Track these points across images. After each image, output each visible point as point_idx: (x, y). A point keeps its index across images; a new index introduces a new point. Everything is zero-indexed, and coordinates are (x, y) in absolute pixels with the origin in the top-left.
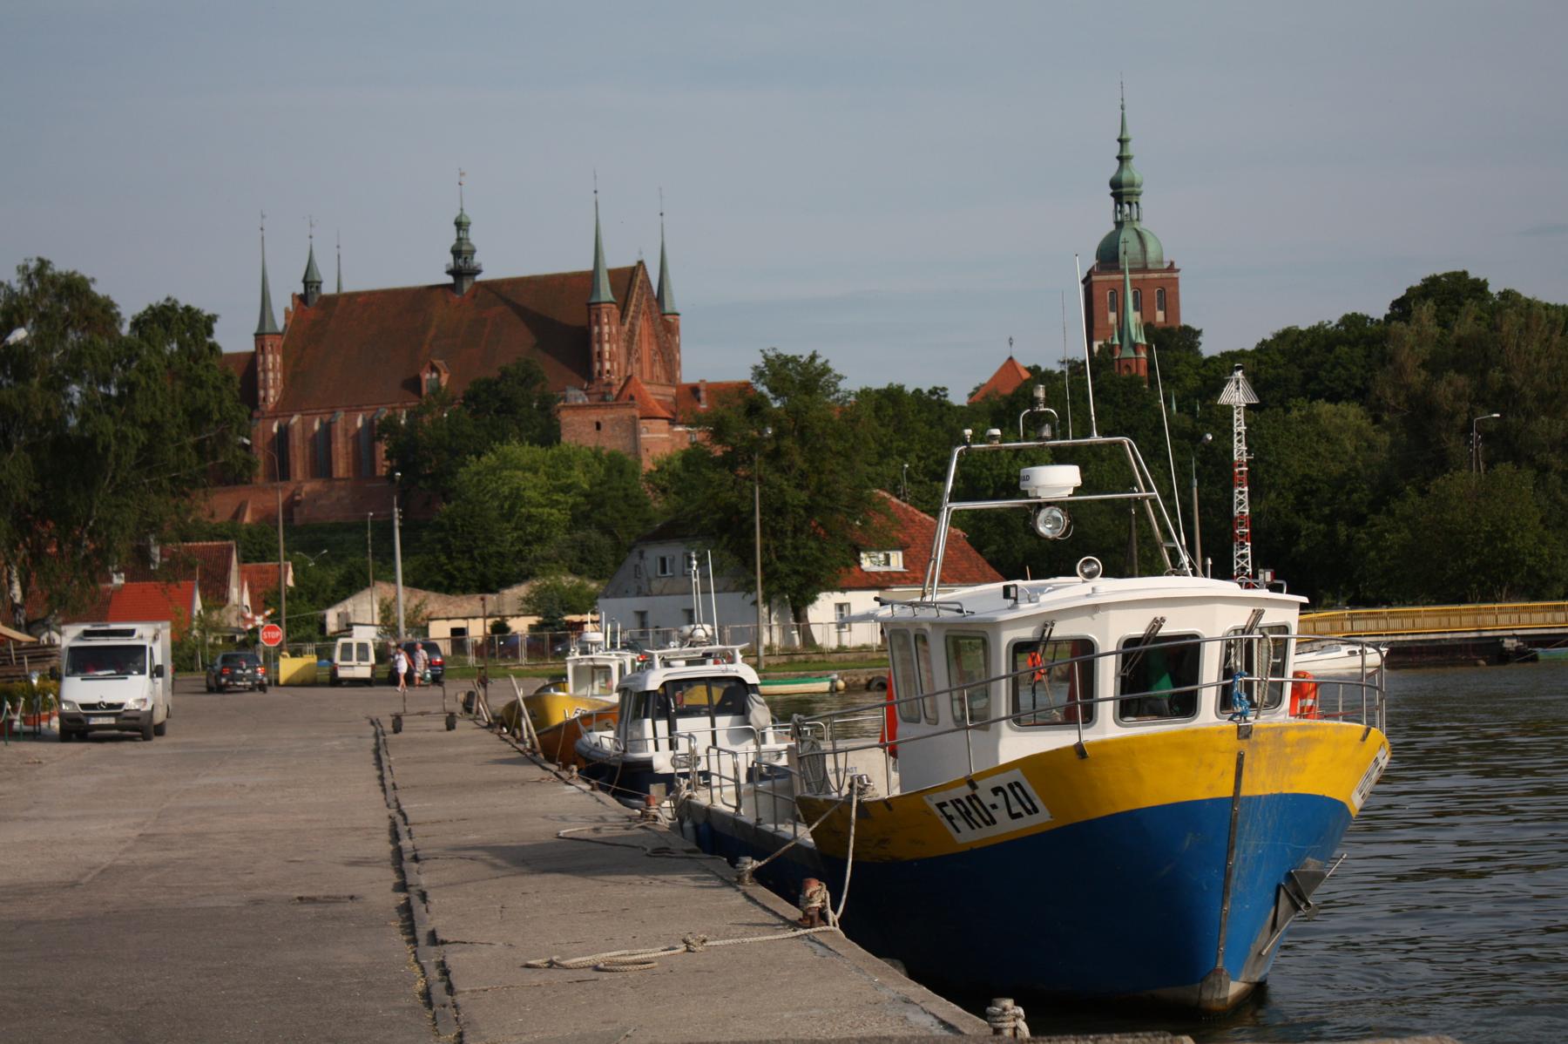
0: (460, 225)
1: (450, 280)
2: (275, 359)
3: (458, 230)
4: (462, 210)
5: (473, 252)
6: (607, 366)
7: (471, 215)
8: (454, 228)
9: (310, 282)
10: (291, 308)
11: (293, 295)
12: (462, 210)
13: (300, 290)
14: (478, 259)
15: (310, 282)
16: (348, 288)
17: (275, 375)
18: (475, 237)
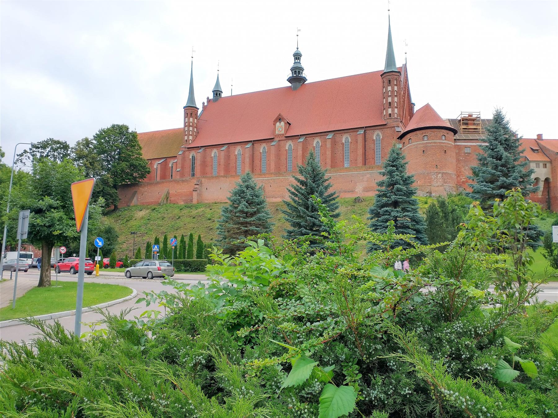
0: (297, 56)
1: (289, 84)
2: (194, 120)
3: (296, 59)
4: (297, 48)
5: (303, 70)
7: (301, 50)
9: (217, 93)
10: (206, 104)
11: (208, 98)
12: (297, 48)
13: (211, 97)
14: (305, 74)
15: (217, 93)
16: (234, 94)
17: (193, 129)
18: (304, 62)
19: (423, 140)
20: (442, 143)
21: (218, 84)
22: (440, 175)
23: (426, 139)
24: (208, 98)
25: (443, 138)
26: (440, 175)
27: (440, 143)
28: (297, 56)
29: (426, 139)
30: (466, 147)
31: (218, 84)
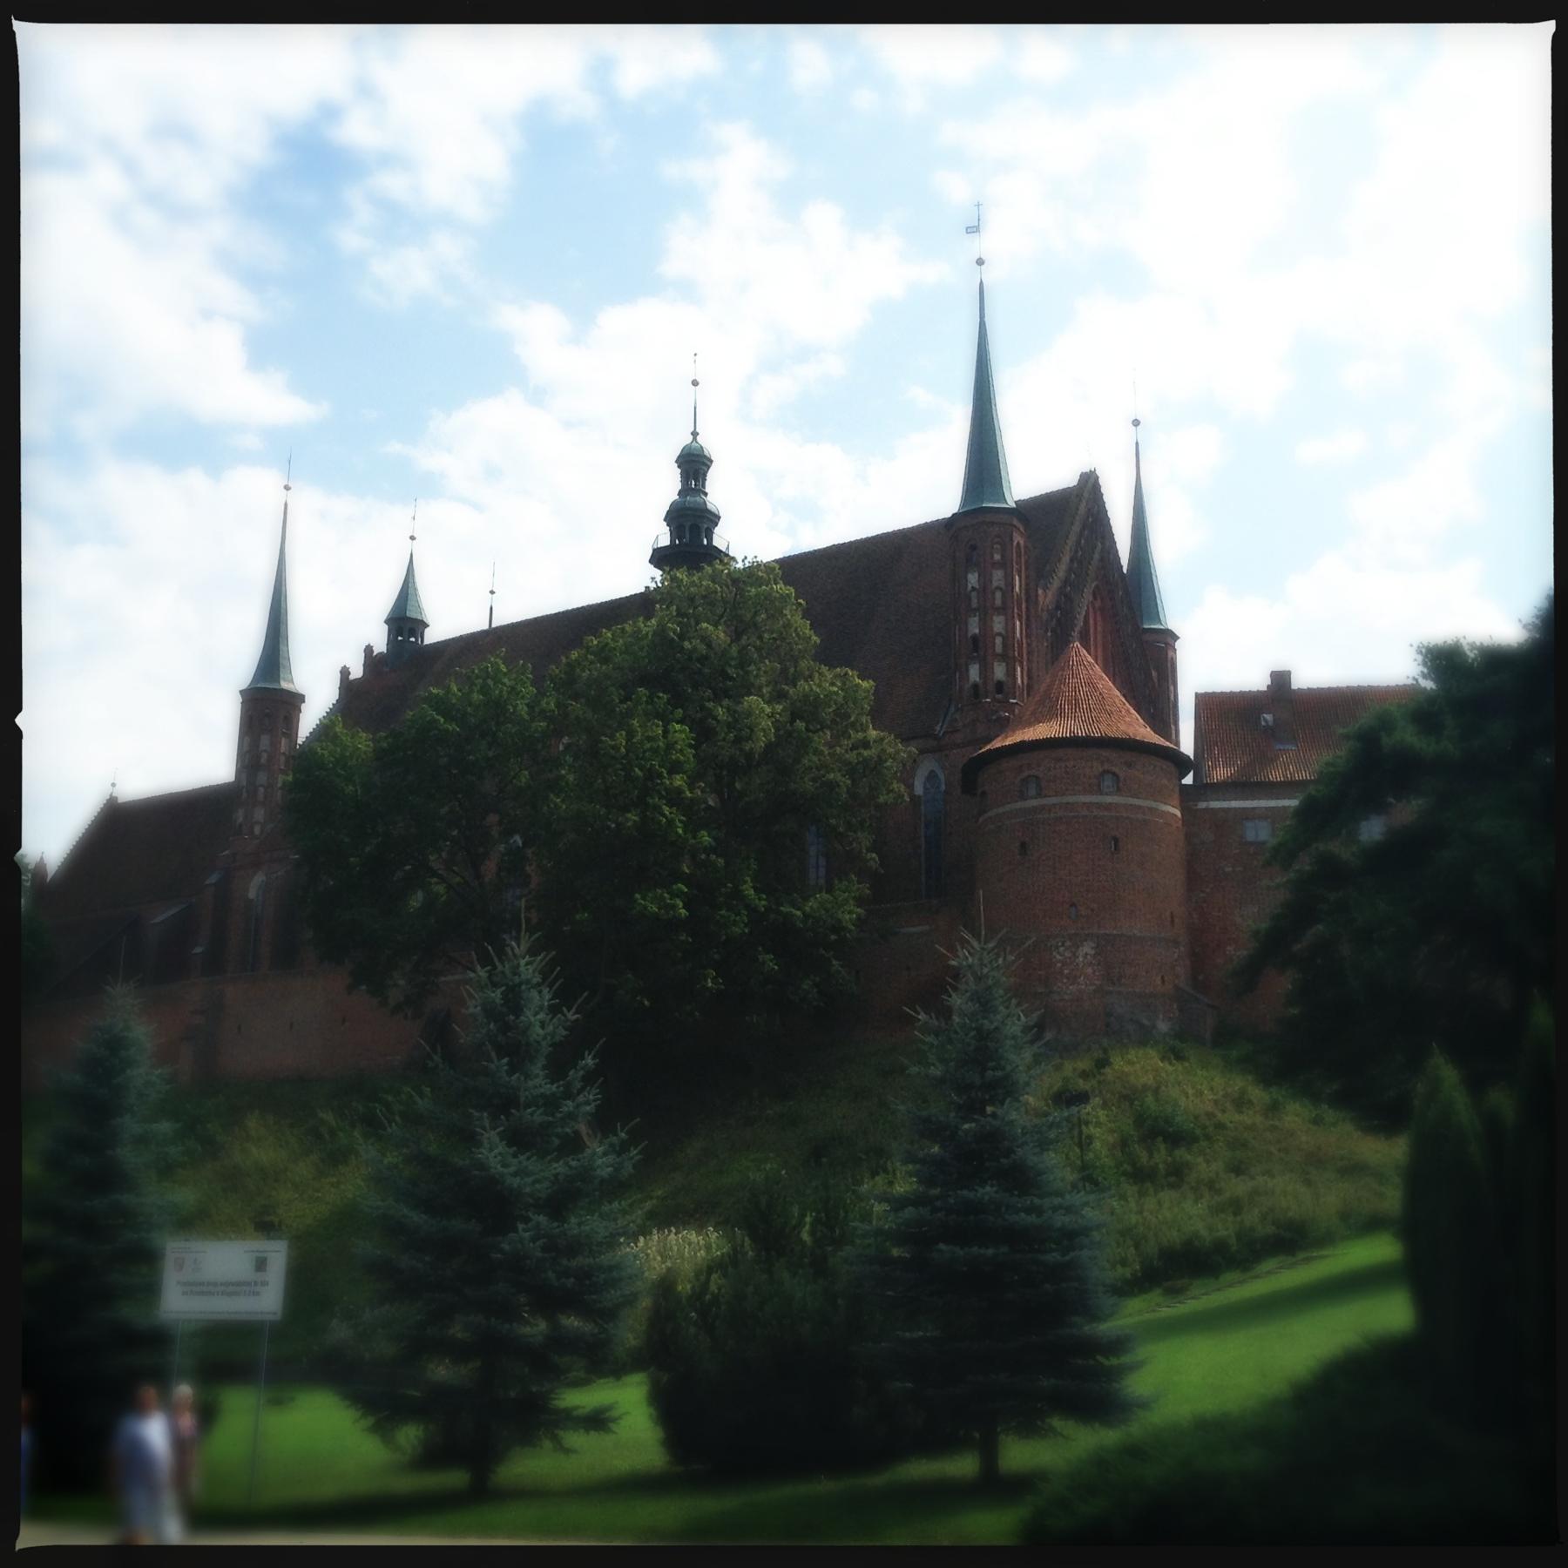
0: (694, 465)
3: (686, 477)
4: (695, 434)
5: (714, 519)
6: (999, 672)
8: (676, 473)
12: (695, 434)
14: (722, 537)
15: (404, 622)
18: (718, 492)
19: (1023, 797)
20: (1099, 806)
21: (407, 592)
22: (1087, 949)
23: (1032, 792)
24: (368, 650)
25: (1108, 782)
26: (1087, 949)
27: (1088, 806)
28: (694, 465)
29: (1032, 792)
30: (1247, 815)
31: (407, 592)
